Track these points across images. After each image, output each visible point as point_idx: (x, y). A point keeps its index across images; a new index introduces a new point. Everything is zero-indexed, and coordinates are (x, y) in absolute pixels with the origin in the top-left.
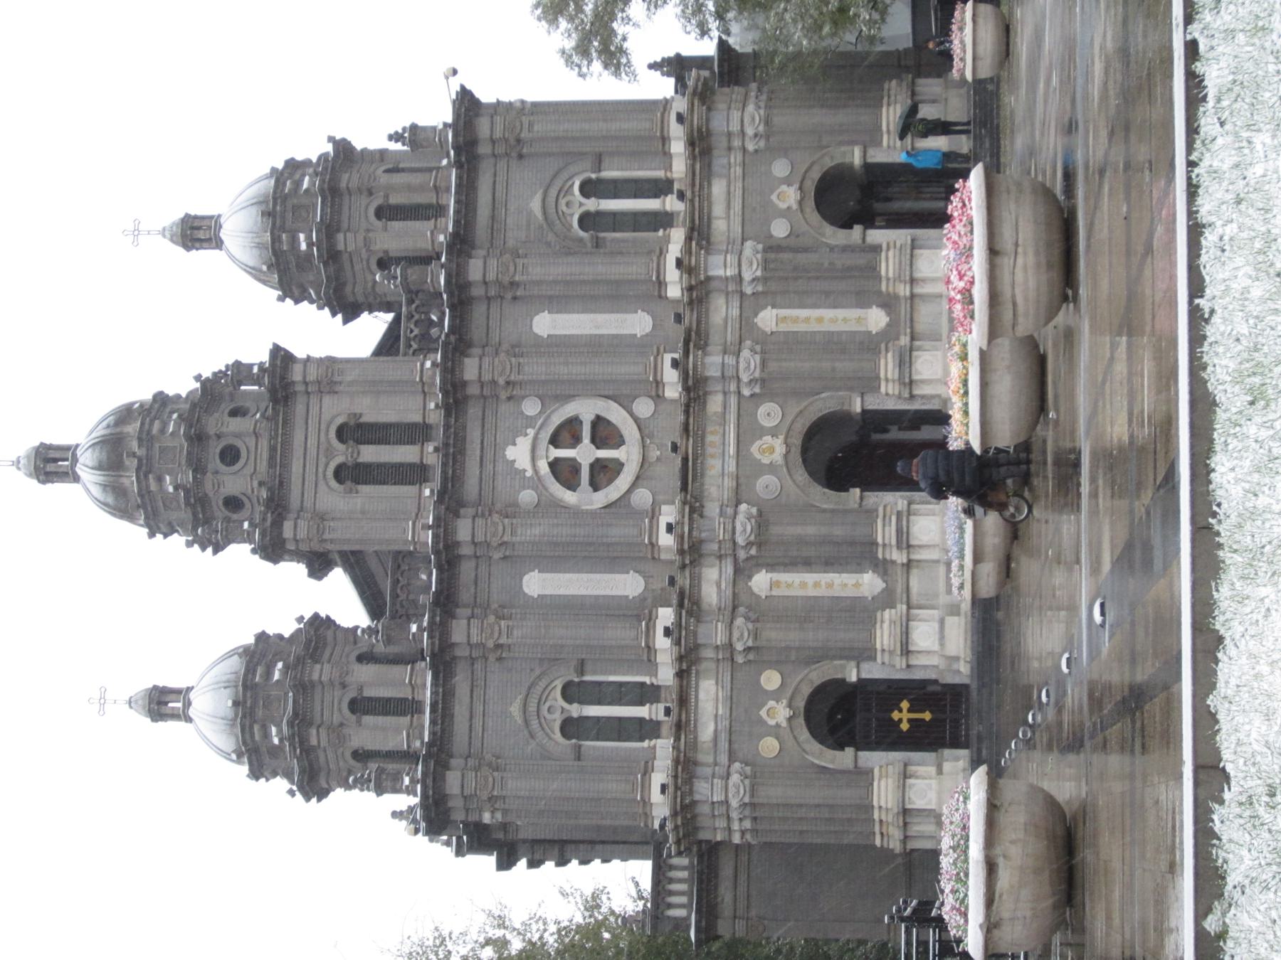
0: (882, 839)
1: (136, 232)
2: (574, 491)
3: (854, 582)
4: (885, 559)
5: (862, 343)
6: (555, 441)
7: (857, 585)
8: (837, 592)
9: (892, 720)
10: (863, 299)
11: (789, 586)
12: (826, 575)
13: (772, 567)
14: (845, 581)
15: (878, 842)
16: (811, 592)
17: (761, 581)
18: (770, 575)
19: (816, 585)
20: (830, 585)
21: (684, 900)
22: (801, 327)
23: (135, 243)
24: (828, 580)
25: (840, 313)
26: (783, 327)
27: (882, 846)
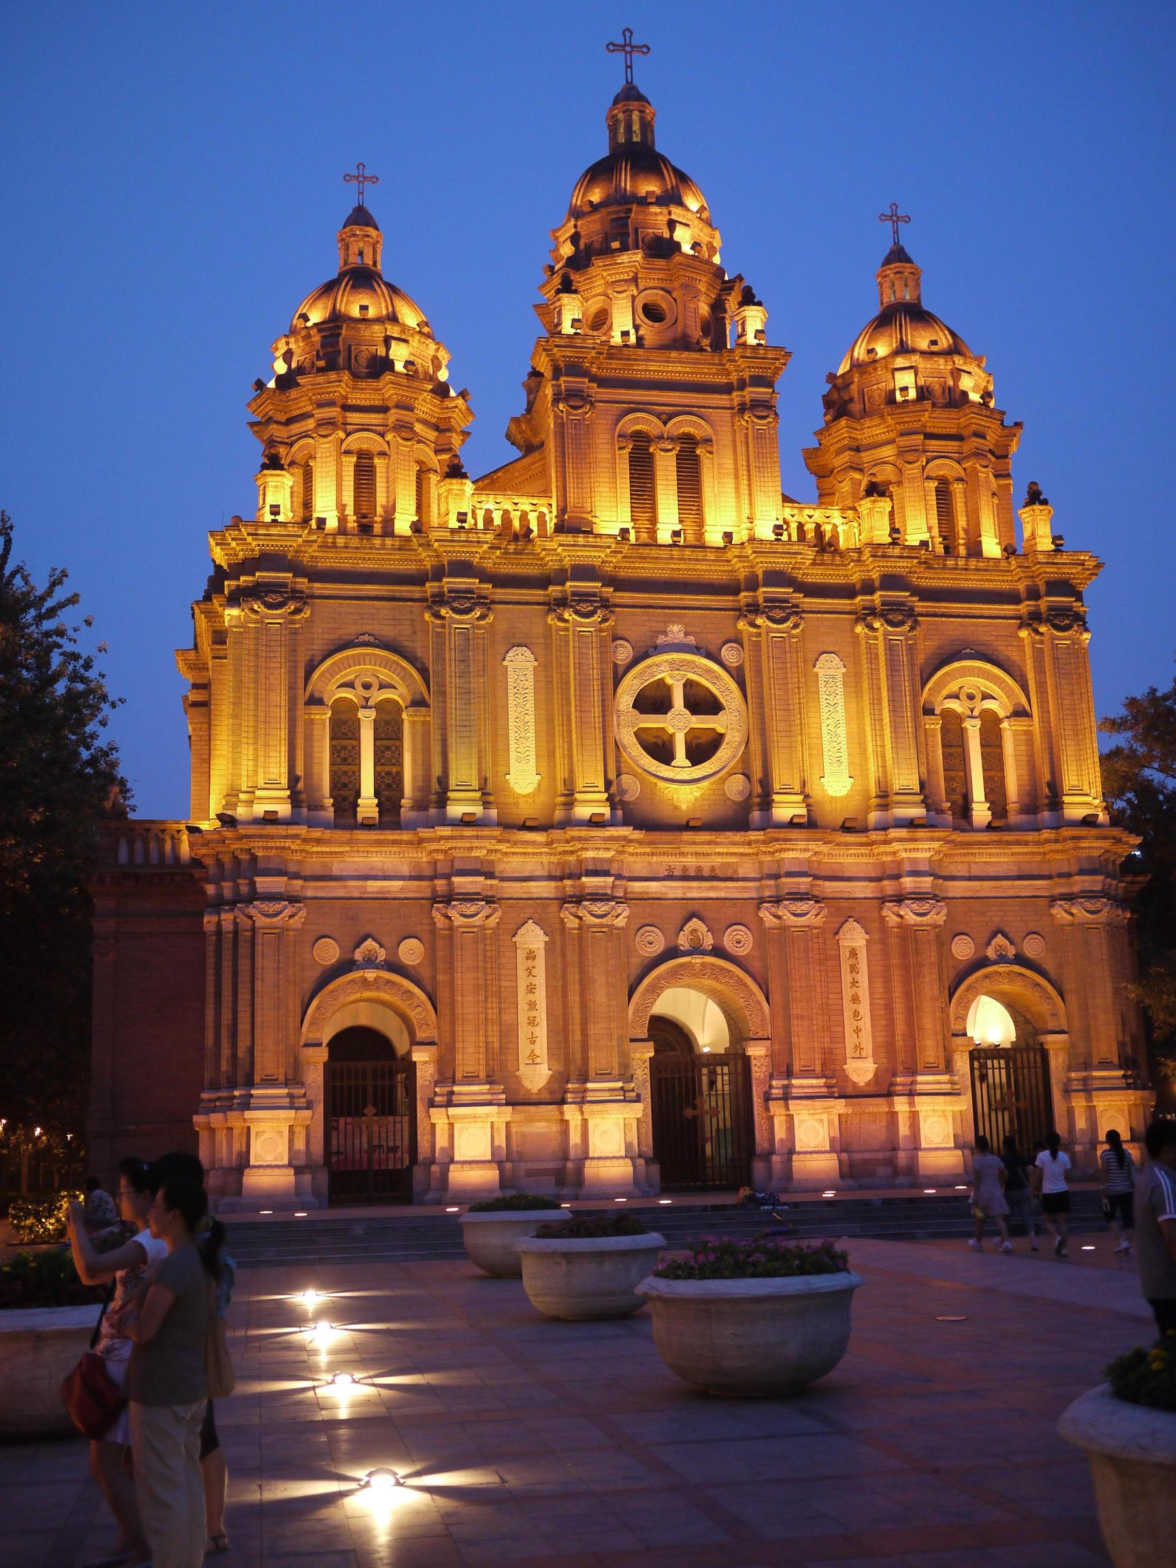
0: (210, 1100)
1: (894, 217)
2: (634, 707)
3: (537, 1052)
4: (566, 1091)
5: (831, 1051)
6: (689, 685)
7: (533, 1055)
8: (524, 1032)
9: (365, 1106)
10: (887, 1048)
11: (530, 972)
12: (544, 1016)
13: (549, 948)
14: (538, 1040)
15: (205, 1096)
16: (522, 998)
17: (533, 938)
18: (542, 945)
19: (532, 1005)
20: (532, 1022)
21: (139, 859)
22: (846, 977)
23: (883, 217)
24: (538, 1020)
25: (866, 1024)
26: (845, 954)
27: (202, 1100)
